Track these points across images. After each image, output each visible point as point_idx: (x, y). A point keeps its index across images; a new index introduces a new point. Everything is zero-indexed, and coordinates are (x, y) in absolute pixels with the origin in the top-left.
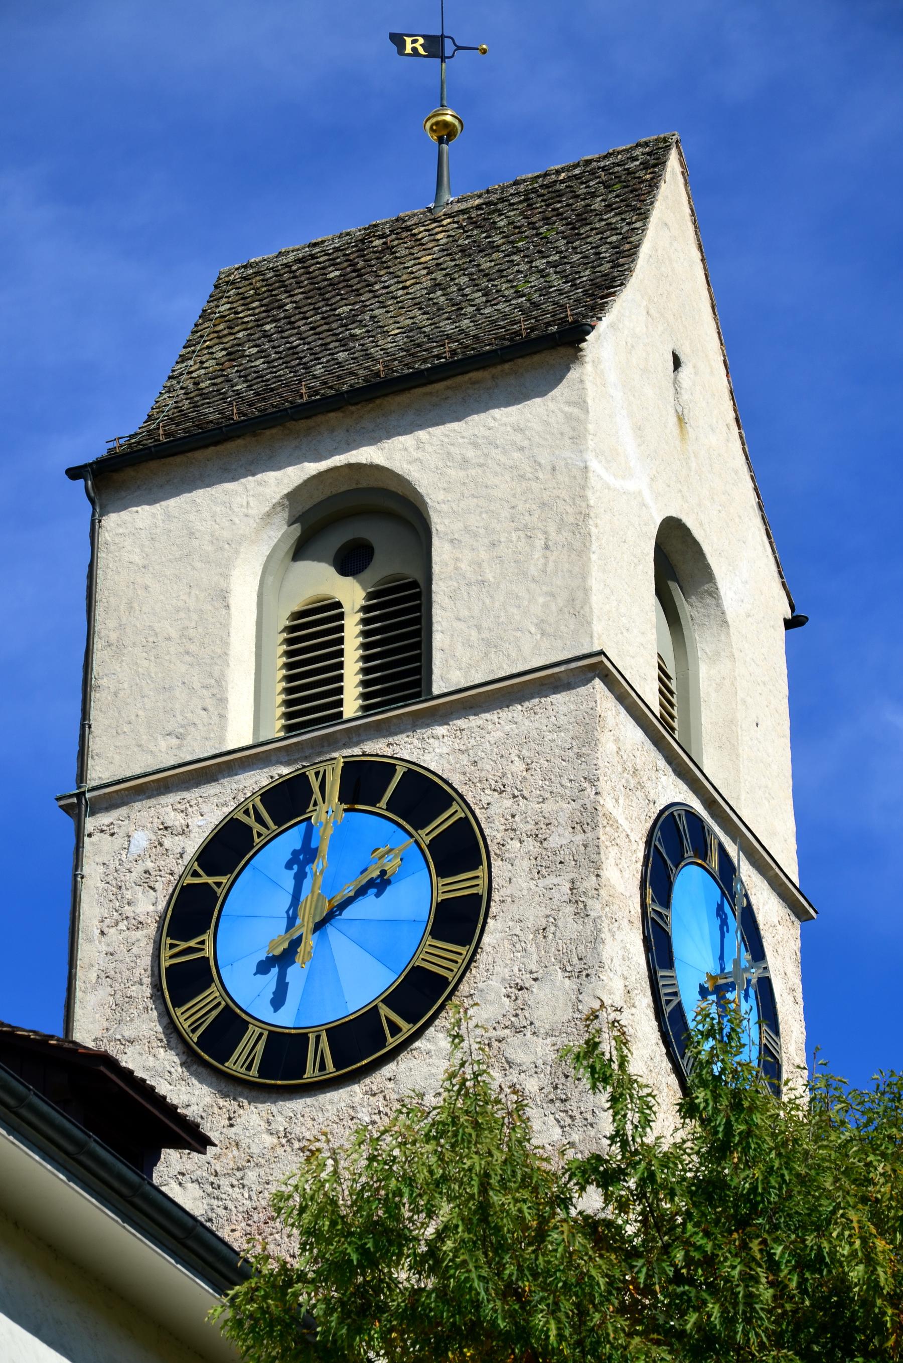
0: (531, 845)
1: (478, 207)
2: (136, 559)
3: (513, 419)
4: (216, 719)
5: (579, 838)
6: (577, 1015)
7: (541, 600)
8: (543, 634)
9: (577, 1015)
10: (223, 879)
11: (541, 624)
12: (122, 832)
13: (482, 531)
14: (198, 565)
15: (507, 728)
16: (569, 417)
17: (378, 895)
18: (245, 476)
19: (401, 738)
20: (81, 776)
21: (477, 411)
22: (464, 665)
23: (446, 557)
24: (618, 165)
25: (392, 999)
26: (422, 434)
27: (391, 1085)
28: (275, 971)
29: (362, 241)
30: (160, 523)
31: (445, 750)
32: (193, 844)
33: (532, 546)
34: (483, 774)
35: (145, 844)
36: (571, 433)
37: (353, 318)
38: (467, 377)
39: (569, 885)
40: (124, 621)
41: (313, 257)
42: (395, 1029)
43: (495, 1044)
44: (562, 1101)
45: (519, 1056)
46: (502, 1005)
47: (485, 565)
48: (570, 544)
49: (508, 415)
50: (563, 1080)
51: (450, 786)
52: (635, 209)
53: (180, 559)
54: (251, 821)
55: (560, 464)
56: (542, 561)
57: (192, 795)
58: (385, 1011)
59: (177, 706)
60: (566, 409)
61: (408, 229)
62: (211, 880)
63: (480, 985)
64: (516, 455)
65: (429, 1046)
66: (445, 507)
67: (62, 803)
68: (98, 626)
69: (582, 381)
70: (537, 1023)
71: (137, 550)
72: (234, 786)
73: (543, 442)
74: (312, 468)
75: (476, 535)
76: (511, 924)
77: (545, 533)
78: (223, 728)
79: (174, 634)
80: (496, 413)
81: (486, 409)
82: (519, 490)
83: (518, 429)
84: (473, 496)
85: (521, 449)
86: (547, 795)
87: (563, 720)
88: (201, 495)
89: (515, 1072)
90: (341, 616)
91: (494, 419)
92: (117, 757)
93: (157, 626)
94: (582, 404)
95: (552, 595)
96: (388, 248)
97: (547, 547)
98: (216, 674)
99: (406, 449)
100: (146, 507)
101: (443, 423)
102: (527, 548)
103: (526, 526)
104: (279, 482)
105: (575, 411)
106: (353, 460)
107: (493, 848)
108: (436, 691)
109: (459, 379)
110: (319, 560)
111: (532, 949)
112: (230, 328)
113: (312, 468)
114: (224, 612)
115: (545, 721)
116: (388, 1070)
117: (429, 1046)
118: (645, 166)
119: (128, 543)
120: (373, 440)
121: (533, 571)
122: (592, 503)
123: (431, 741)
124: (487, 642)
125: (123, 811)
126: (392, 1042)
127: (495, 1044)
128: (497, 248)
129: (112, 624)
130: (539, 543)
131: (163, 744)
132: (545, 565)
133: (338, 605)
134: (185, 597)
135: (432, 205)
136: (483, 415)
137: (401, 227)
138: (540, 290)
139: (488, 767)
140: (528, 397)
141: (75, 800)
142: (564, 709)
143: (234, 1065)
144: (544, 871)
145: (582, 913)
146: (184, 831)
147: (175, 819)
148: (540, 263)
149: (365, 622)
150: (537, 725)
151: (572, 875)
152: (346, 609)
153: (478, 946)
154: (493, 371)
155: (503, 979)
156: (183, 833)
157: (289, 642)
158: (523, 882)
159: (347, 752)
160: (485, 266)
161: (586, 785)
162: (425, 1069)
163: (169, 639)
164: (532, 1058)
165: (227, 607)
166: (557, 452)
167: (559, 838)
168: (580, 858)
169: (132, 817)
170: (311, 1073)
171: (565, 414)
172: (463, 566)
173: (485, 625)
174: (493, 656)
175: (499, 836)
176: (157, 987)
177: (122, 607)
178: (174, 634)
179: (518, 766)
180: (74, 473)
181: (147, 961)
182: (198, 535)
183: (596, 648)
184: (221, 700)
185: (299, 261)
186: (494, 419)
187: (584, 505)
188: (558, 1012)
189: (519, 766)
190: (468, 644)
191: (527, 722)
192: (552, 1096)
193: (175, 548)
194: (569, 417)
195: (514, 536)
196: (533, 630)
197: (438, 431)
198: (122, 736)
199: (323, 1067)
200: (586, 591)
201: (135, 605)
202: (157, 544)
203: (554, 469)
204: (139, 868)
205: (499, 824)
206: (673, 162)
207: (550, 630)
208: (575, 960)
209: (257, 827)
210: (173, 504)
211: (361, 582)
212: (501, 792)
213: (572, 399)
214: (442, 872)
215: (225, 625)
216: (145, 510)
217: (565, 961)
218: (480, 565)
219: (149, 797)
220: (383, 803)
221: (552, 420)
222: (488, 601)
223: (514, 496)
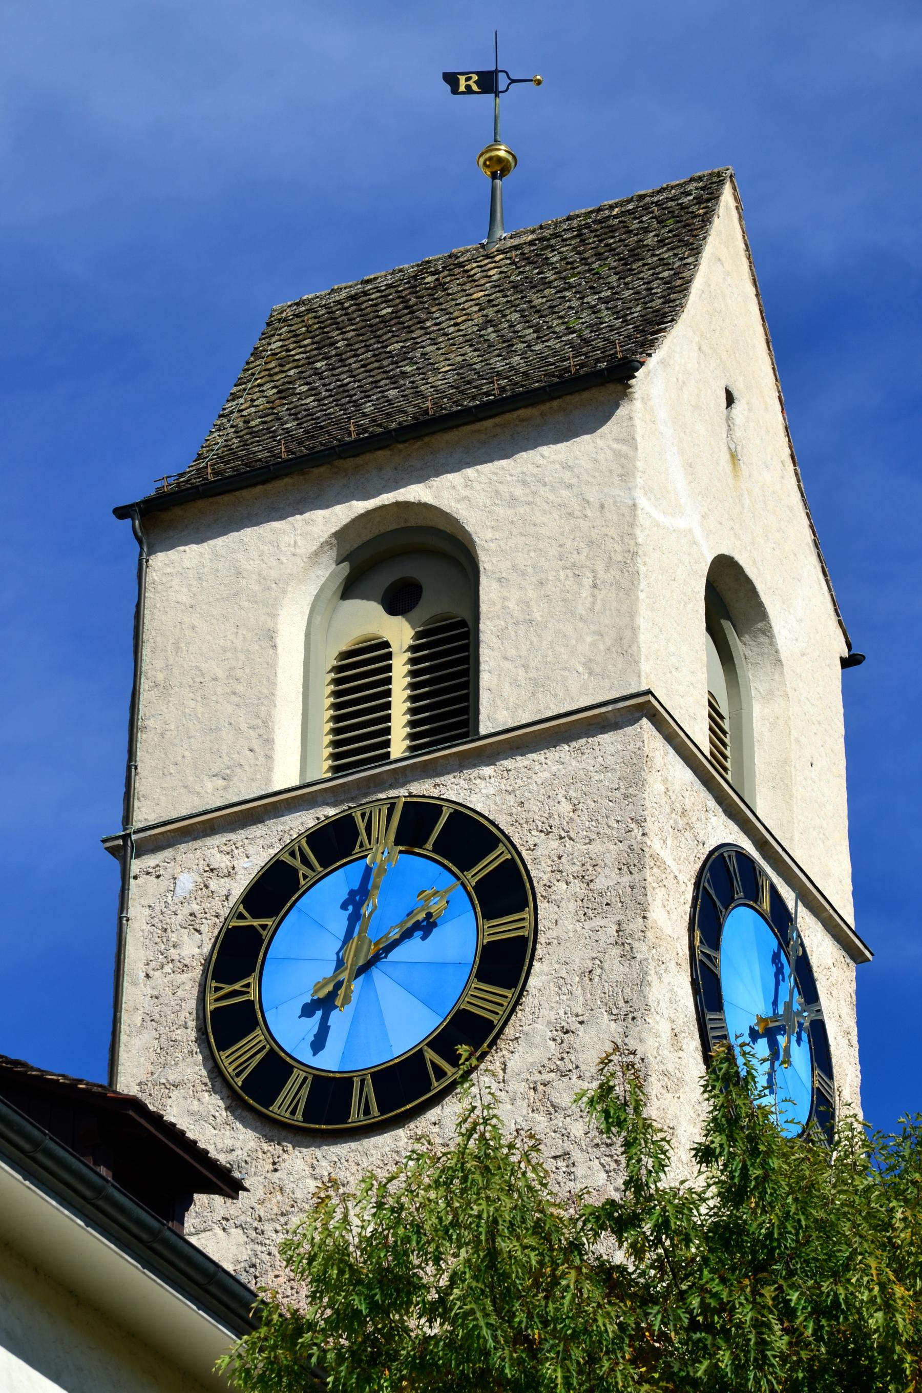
0: (577, 887)
1: (531, 243)
2: (184, 598)
3: (561, 457)
4: (262, 760)
5: (626, 879)
7: (589, 639)
8: (590, 674)
10: (269, 922)
11: (588, 663)
12: (167, 874)
13: (530, 570)
14: (246, 605)
15: (554, 768)
16: (618, 455)
17: (424, 938)
18: (293, 515)
19: (448, 779)
20: (127, 818)
21: (525, 449)
22: (511, 705)
23: (493, 596)
24: (672, 200)
26: (470, 472)
27: (435, 1129)
28: (319, 1014)
29: (415, 277)
30: (207, 563)
31: (492, 791)
32: (238, 887)
33: (580, 585)
34: (530, 815)
35: (191, 886)
36: (620, 471)
37: (404, 356)
38: (515, 415)
39: (615, 927)
40: (171, 662)
41: (365, 293)
43: (540, 1088)
44: (608, 1145)
46: (547, 1049)
47: (533, 603)
48: (618, 583)
51: (497, 827)
52: (687, 244)
54: (297, 863)
55: (609, 502)
56: (590, 599)
57: (238, 836)
59: (224, 747)
61: (461, 265)
62: (256, 923)
63: (526, 1028)
64: (565, 493)
66: (492, 546)
67: (108, 844)
68: (146, 666)
69: (631, 418)
70: (583, 1067)
71: (185, 590)
72: (281, 828)
74: (360, 507)
75: (524, 574)
76: (557, 966)
77: (593, 571)
78: (269, 770)
79: (221, 674)
80: (545, 450)
81: (534, 447)
82: (567, 528)
83: (567, 467)
84: (521, 534)
85: (570, 487)
87: (610, 760)
88: (248, 534)
90: (389, 656)
91: (543, 456)
92: (163, 799)
93: (203, 666)
94: (631, 441)
95: (601, 634)
96: (440, 285)
97: (595, 586)
98: (263, 715)
99: (454, 487)
100: (194, 546)
101: (491, 461)
102: (575, 587)
103: (574, 565)
104: (326, 521)
105: (624, 448)
106: (401, 499)
107: (539, 889)
108: (483, 731)
109: (508, 417)
110: (369, 599)
111: (578, 992)
112: (281, 365)
113: (360, 507)
114: (271, 652)
115: (592, 762)
118: (699, 200)
119: (175, 582)
121: (581, 610)
122: (640, 541)
123: (478, 781)
124: (535, 682)
125: (169, 853)
126: (437, 1086)
127: (540, 1088)
128: (549, 285)
129: (159, 664)
130: (587, 581)
131: (209, 785)
132: (593, 603)
133: (386, 645)
134: (232, 637)
135: (485, 241)
137: (454, 264)
138: (591, 326)
139: (535, 808)
140: (577, 435)
141: (121, 842)
142: (611, 749)
143: (279, 1109)
144: (590, 913)
145: (628, 956)
146: (230, 874)
147: (221, 861)
148: (592, 299)
149: (412, 661)
150: (584, 765)
151: (619, 917)
152: (394, 648)
153: (523, 988)
155: (549, 1023)
157: (337, 682)
158: (569, 924)
161: (633, 826)
163: (215, 679)
165: (275, 647)
166: (606, 490)
169: (178, 859)
170: (356, 1117)
171: (614, 451)
172: (511, 605)
173: (532, 665)
175: (545, 877)
176: (201, 1030)
178: (221, 674)
180: (122, 513)
181: (192, 1004)
182: (245, 574)
183: (644, 688)
184: (267, 740)
185: (352, 298)
186: (543, 456)
189: (566, 807)
190: (515, 683)
191: (574, 763)
192: (597, 1141)
193: (222, 588)
194: (618, 455)
195: (562, 575)
196: (581, 669)
198: (169, 778)
199: (367, 1112)
200: (634, 630)
201: (182, 645)
202: (205, 584)
203: (602, 507)
204: (184, 911)
205: (545, 865)
206: (727, 196)
207: (598, 670)
208: (621, 1003)
209: (303, 870)
211: (408, 620)
212: (548, 834)
215: (272, 666)
217: (611, 1004)
218: (527, 603)
219: (195, 839)
220: (429, 845)
221: (601, 457)
222: (535, 640)
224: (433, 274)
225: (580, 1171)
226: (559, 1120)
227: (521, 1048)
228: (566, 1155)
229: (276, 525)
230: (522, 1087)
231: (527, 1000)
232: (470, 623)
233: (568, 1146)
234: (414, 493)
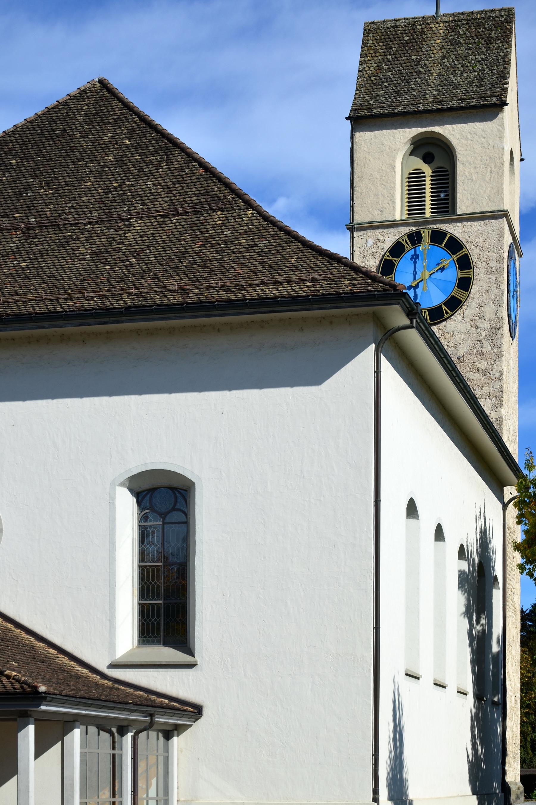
0: (485, 264)
1: (452, 22)
2: (366, 149)
3: (482, 127)
4: (392, 208)
5: (498, 265)
6: (496, 316)
7: (489, 189)
8: (489, 200)
9: (496, 316)
11: (489, 197)
12: (364, 239)
13: (472, 163)
14: (385, 155)
15: (479, 227)
16: (498, 130)
17: (441, 272)
18: (400, 128)
19: (448, 225)
22: (466, 205)
23: (461, 169)
24: (497, 17)
25: (446, 303)
26: (454, 126)
27: (445, 328)
28: (412, 290)
29: (413, 25)
30: (373, 139)
31: (461, 231)
32: (387, 246)
33: (487, 171)
34: (471, 240)
35: (372, 243)
36: (499, 136)
37: (418, 62)
38: (469, 111)
39: (495, 278)
40: (363, 170)
41: (397, 27)
42: (447, 313)
43: (474, 321)
44: (492, 340)
45: (480, 325)
46: (476, 310)
47: (473, 174)
48: (498, 173)
49: (480, 125)
50: (492, 334)
51: (462, 242)
52: (507, 42)
53: (380, 152)
54: (404, 243)
55: (496, 146)
56: (490, 176)
57: (386, 231)
58: (444, 307)
59: (380, 201)
60: (498, 127)
61: (429, 24)
62: (391, 258)
63: (470, 303)
64: (483, 139)
65: (456, 319)
66: (461, 152)
67: (347, 227)
68: (355, 170)
69: (503, 119)
70: (485, 317)
71: (366, 146)
72: (398, 230)
73: (491, 137)
74: (421, 130)
76: (479, 287)
77: (491, 167)
79: (378, 177)
80: (477, 124)
81: (474, 122)
82: (483, 152)
83: (483, 131)
85: (484, 138)
86: (490, 250)
87: (495, 228)
88: (385, 132)
89: (479, 329)
90: (424, 177)
91: (476, 126)
92: (362, 214)
93: (373, 173)
95: (492, 188)
96: (423, 32)
97: (491, 172)
98: (392, 193)
99: (449, 130)
100: (368, 132)
101: (461, 124)
102: (485, 171)
103: (485, 164)
105: (500, 128)
106: (433, 130)
108: (459, 211)
109: (467, 111)
111: (485, 295)
113: (421, 130)
114: (394, 173)
115: (489, 228)
116: (444, 323)
117: (456, 319)
119: (363, 143)
120: (439, 125)
121: (487, 179)
122: (504, 160)
123: (457, 227)
124: (473, 199)
125: (365, 232)
127: (474, 321)
129: (359, 170)
130: (489, 170)
131: (376, 212)
132: (491, 178)
134: (381, 166)
136: (473, 124)
139: (473, 239)
140: (487, 121)
141: (351, 227)
142: (495, 225)
144: (488, 273)
146: (384, 242)
147: (381, 237)
150: (487, 228)
151: (496, 276)
152: (426, 174)
153: (470, 292)
154: (477, 110)
155: (476, 303)
156: (383, 242)
158: (482, 275)
159: (432, 226)
160: (460, 52)
161: (501, 249)
162: (454, 325)
163: (377, 178)
164: (484, 326)
165: (395, 171)
166: (495, 141)
167: (493, 264)
168: (499, 271)
169: (368, 234)
171: (497, 129)
172: (466, 173)
173: (473, 194)
174: (475, 204)
175: (476, 260)
177: (362, 165)
178: (378, 177)
179: (481, 240)
182: (385, 145)
183: (505, 209)
184: (393, 202)
186: (476, 126)
187: (502, 161)
188: (491, 315)
189: (482, 240)
190: (467, 198)
191: (484, 227)
192: (489, 338)
193: (378, 148)
194: (498, 130)
196: (487, 198)
197: (459, 126)
198: (363, 208)
200: (502, 189)
201: (366, 165)
202: (372, 146)
203: (494, 147)
204: (370, 251)
205: (476, 256)
207: (492, 199)
208: (496, 301)
209: (406, 245)
210: (377, 133)
212: (476, 247)
213: (500, 124)
214: (461, 268)
216: (368, 133)
217: (493, 300)
219: (373, 229)
220: (443, 245)
221: (494, 130)
222: (473, 186)
223: (482, 153)
224: (420, 25)
225: (484, 346)
226: (479, 331)
227: (468, 308)
228: (480, 341)
229: (394, 131)
230: (469, 320)
231: (471, 295)
232: (450, 172)
233: (482, 339)
234: (436, 129)
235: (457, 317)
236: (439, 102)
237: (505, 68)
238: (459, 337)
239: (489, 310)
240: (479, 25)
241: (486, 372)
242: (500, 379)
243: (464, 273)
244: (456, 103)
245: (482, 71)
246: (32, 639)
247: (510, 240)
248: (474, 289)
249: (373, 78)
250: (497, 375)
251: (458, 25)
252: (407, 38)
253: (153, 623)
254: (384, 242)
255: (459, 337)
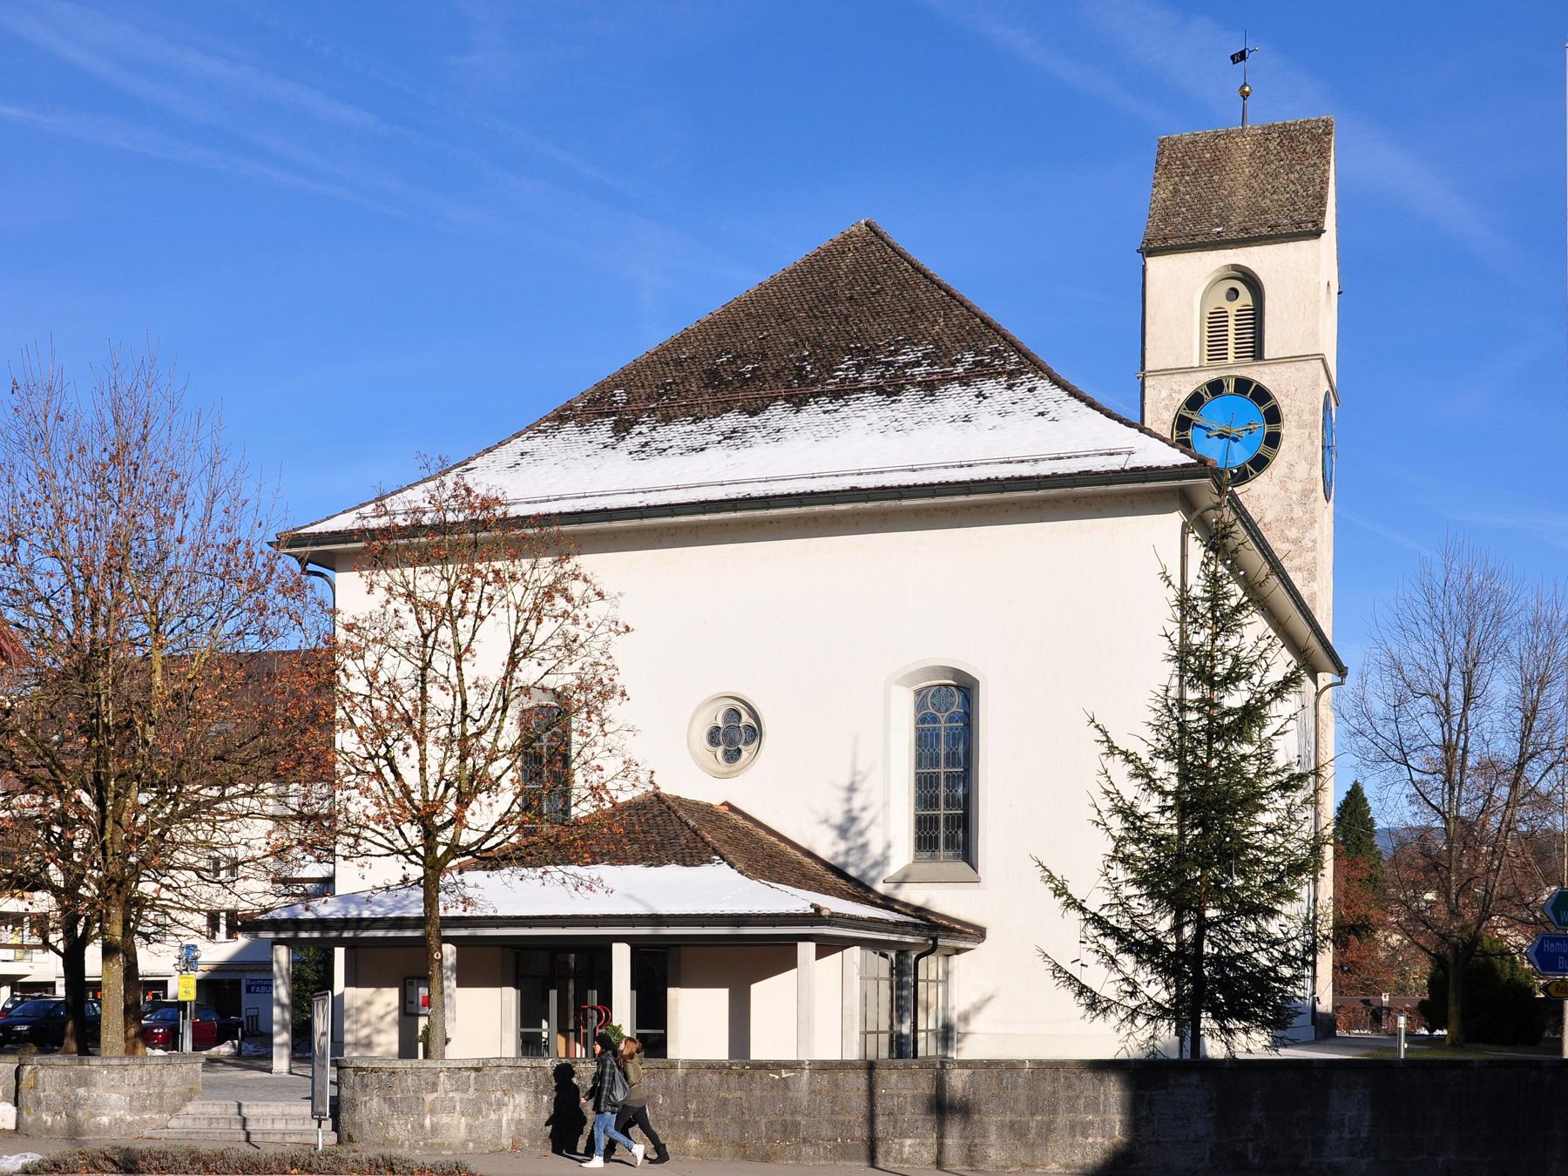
0: (1296, 417)
20: (1143, 368)
32: (1184, 397)
42: (1252, 473)
54: (1203, 394)
58: (1248, 467)
116: (1248, 485)
146: (1180, 392)
147: (1176, 387)
158: (1294, 430)
204: (1164, 403)
225: (1295, 511)
235: (1263, 478)
236: (1246, 230)
237: (1322, 188)
238: (1265, 503)
239: (1301, 470)
240: (1292, 139)
241: (1296, 542)
242: (1313, 549)
243: (1273, 428)
244: (1265, 231)
245: (1296, 192)
246: (799, 854)
247: (1327, 388)
248: (1284, 445)
249: (1168, 203)
250: (1310, 544)
251: (1267, 139)
252: (1208, 155)
253: (931, 836)
254: (1180, 392)
255: (1265, 503)
